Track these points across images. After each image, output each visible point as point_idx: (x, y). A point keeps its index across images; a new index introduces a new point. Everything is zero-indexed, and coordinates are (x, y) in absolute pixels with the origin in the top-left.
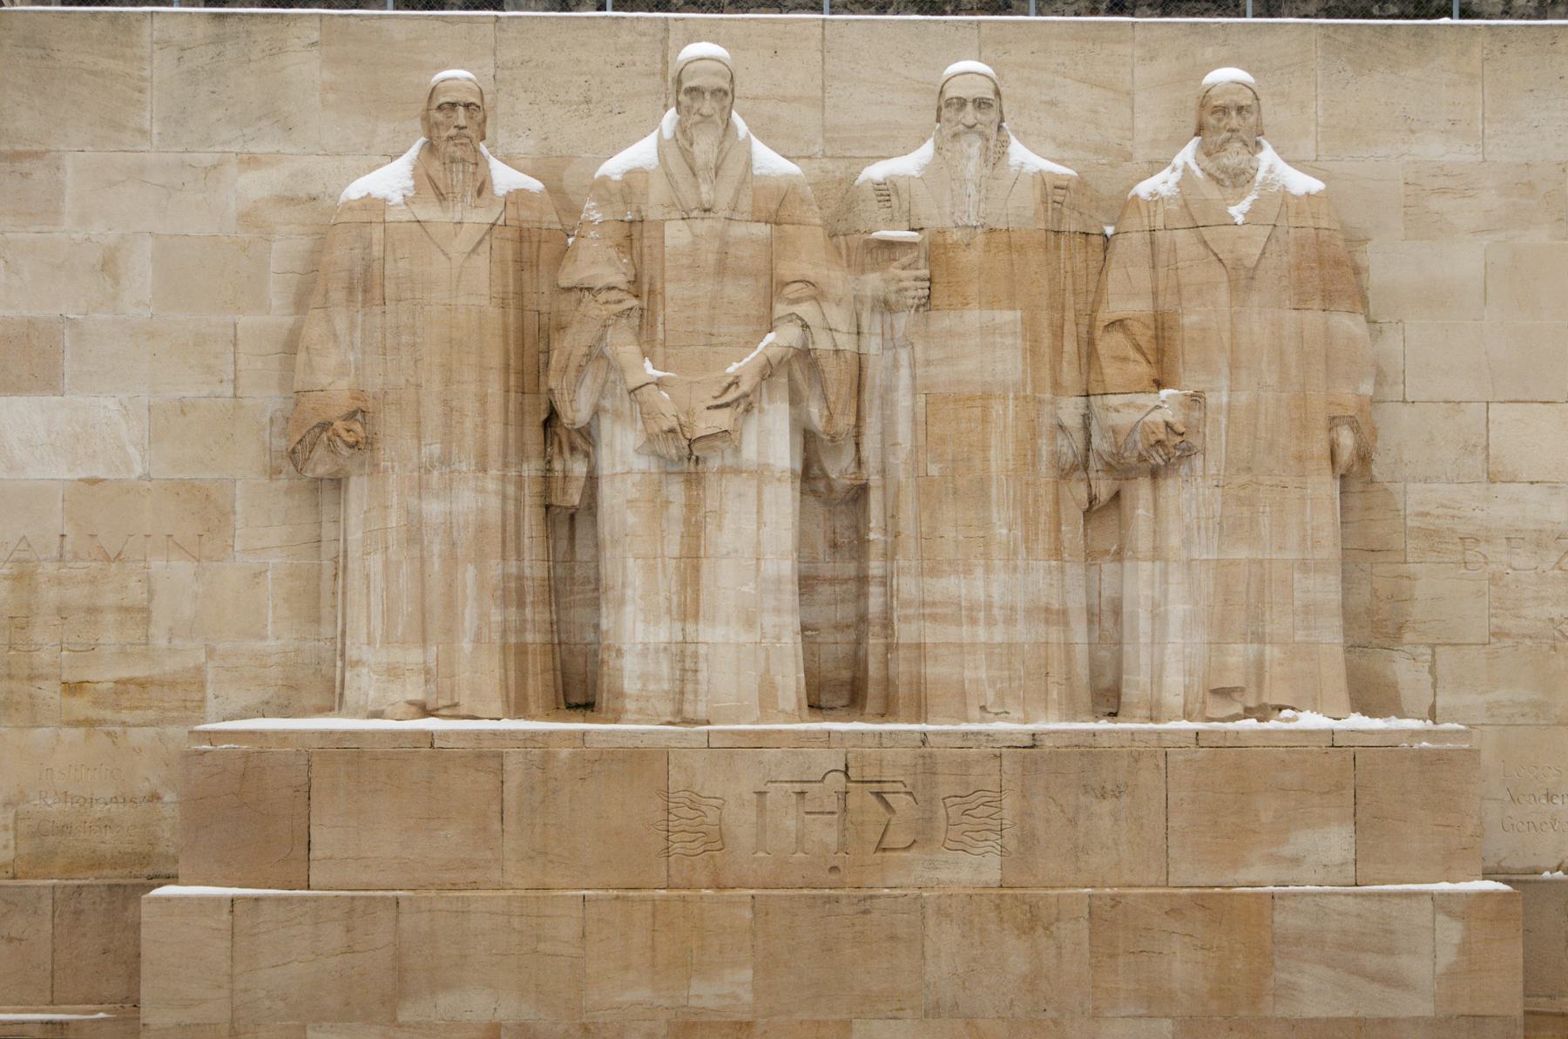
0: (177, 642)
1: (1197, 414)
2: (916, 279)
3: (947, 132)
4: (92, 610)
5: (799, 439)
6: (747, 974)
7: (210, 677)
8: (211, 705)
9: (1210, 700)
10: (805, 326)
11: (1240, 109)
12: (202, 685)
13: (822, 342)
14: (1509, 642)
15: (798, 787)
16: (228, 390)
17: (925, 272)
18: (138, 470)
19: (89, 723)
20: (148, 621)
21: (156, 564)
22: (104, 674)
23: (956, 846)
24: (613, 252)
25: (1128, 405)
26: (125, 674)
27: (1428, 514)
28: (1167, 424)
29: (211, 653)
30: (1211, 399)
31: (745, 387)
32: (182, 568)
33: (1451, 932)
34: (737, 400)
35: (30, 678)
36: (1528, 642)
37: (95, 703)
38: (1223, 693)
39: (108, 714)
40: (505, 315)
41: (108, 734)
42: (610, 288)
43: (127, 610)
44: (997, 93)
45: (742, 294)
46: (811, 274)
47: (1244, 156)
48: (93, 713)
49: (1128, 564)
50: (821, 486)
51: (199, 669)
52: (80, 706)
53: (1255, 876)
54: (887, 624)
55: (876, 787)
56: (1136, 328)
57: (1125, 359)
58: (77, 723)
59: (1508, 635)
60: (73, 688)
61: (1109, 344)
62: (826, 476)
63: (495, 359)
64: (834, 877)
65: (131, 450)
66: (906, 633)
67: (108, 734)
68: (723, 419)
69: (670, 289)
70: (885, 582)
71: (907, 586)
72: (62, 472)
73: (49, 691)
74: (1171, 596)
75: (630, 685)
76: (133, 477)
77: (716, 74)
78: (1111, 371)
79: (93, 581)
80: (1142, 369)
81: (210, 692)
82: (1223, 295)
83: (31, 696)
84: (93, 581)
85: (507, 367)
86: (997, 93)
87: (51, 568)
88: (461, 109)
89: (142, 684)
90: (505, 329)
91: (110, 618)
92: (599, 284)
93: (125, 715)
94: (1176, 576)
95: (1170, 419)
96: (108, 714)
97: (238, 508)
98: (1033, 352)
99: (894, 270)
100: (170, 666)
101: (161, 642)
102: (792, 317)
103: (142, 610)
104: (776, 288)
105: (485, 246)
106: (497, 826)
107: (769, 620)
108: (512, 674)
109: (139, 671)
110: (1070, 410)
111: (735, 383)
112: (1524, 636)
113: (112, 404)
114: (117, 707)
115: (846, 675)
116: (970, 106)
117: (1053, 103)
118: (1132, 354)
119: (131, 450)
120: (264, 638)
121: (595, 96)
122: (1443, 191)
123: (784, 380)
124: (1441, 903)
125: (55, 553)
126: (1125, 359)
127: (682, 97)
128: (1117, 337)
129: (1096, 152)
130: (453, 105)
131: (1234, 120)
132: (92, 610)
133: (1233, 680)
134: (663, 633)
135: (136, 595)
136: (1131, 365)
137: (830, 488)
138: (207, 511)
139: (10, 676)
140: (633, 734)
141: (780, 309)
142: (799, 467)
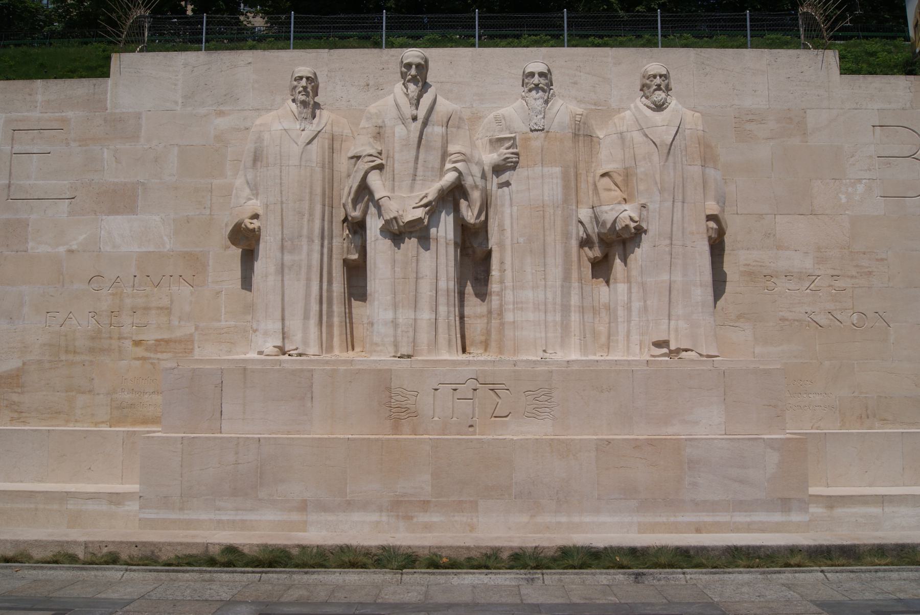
0: (182, 323)
1: (645, 213)
2: (513, 153)
3: (526, 90)
5: (459, 228)
7: (196, 338)
8: (197, 351)
9: (653, 347)
10: (460, 173)
11: (661, 76)
12: (193, 342)
13: (468, 182)
14: (787, 323)
15: (454, 386)
16: (208, 212)
17: (515, 150)
18: (168, 247)
19: (144, 359)
20: (170, 314)
21: (174, 288)
22: (150, 336)
23: (530, 415)
24: (371, 140)
25: (612, 210)
26: (160, 337)
27: (749, 265)
28: (631, 219)
29: (197, 328)
30: (651, 206)
31: (430, 198)
32: (186, 290)
33: (773, 458)
34: (425, 206)
35: (119, 339)
36: (797, 323)
37: (146, 350)
38: (658, 344)
39: (152, 355)
40: (324, 171)
41: (152, 364)
42: (371, 155)
43: (161, 308)
44: (549, 70)
45: (433, 158)
46: (463, 151)
47: (663, 95)
49: (612, 286)
50: (470, 252)
51: (191, 335)
52: (140, 352)
53: (675, 431)
54: (501, 314)
55: (492, 386)
56: (615, 175)
57: (610, 190)
59: (787, 320)
60: (137, 343)
62: (472, 247)
63: (318, 190)
64: (471, 429)
65: (165, 238)
66: (509, 317)
67: (152, 364)
68: (420, 213)
69: (397, 156)
70: (500, 294)
71: (509, 296)
72: (135, 248)
73: (128, 344)
74: (633, 299)
76: (166, 250)
77: (418, 56)
78: (604, 195)
79: (147, 296)
80: (617, 193)
81: (196, 346)
82: (656, 158)
83: (119, 347)
84: (147, 296)
85: (324, 194)
86: (549, 70)
87: (129, 290)
88: (304, 79)
89: (167, 342)
90: (324, 178)
91: (154, 312)
92: (364, 154)
93: (159, 356)
94: (634, 290)
95: (633, 215)
96: (152, 355)
97: (211, 263)
98: (566, 187)
99: (503, 150)
100: (178, 334)
102: (455, 169)
103: (167, 309)
104: (445, 155)
105: (316, 141)
106: (309, 404)
107: (442, 309)
108: (324, 335)
109: (166, 336)
110: (584, 214)
111: (426, 196)
112: (794, 320)
113: (157, 218)
114: (156, 352)
115: (483, 338)
116: (536, 76)
117: (575, 83)
118: (613, 187)
119: (165, 238)
120: (220, 321)
121: (371, 83)
122: (751, 121)
123: (451, 199)
124: (771, 444)
125: (131, 284)
126: (610, 190)
127: (404, 69)
128: (606, 179)
129: (595, 104)
130: (301, 78)
131: (658, 80)
132: (147, 309)
133: (663, 337)
134: (389, 315)
135: (166, 302)
136: (613, 193)
137: (474, 252)
138: (194, 265)
139: (111, 338)
140: (375, 361)
141: (448, 166)
142: (459, 241)
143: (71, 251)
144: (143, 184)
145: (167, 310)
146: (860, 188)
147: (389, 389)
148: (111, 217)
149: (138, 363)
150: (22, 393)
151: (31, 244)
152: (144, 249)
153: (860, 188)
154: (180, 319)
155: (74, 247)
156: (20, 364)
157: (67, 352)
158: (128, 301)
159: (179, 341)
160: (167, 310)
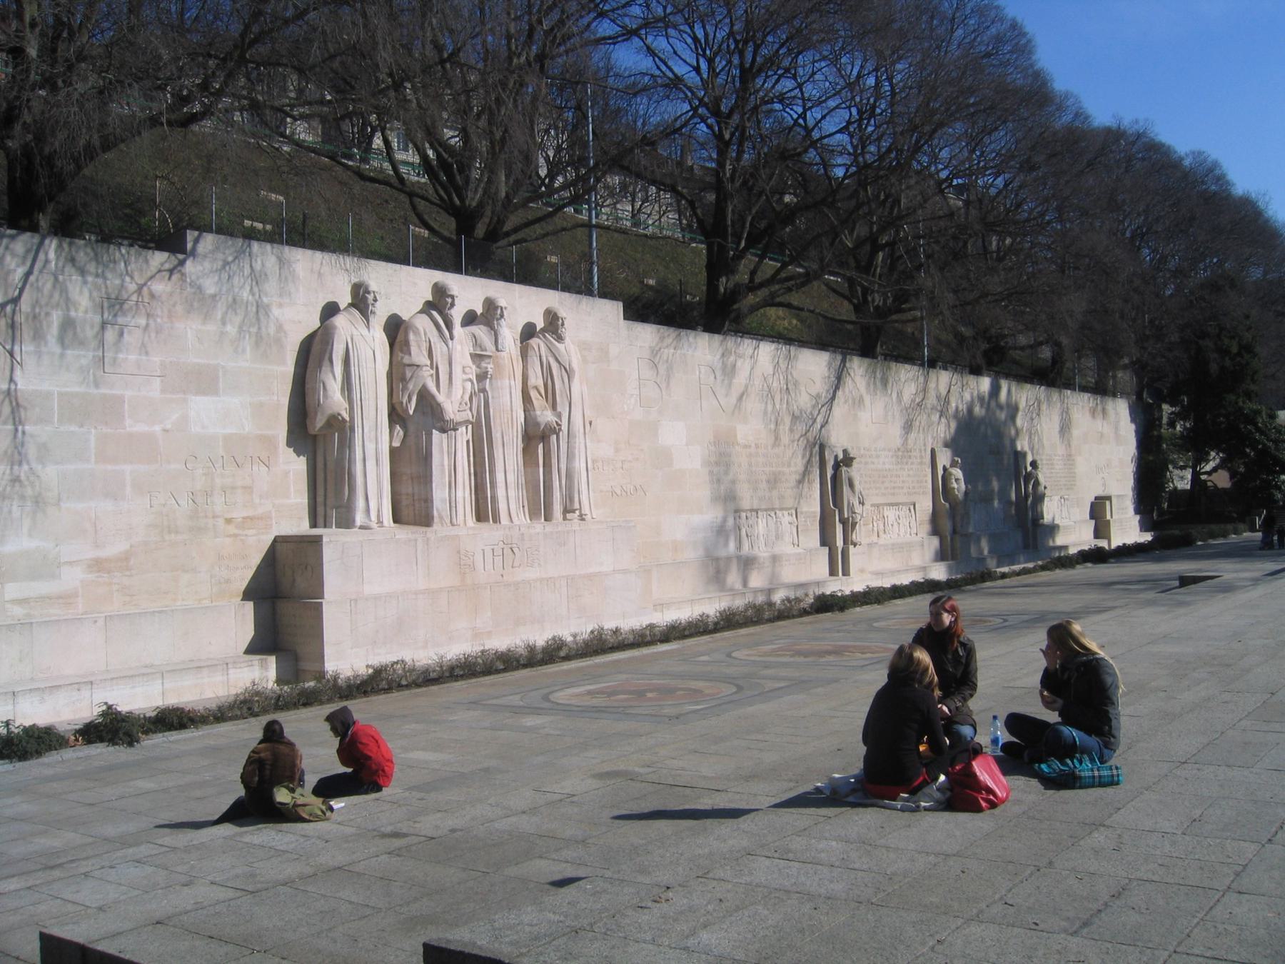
4: (233, 488)
6: (489, 614)
19: (236, 536)
22: (238, 514)
26: (245, 514)
48: (236, 531)
52: (232, 529)
58: (229, 536)
60: (229, 521)
61: (533, 394)
73: (221, 522)
75: (435, 513)
89: (251, 518)
93: (247, 532)
100: (260, 511)
101: (257, 501)
109: (250, 513)
143: (166, 431)
144: (223, 367)
145: (248, 489)
146: (633, 401)
147: (459, 552)
148: (198, 398)
149: (228, 540)
150: (131, 576)
151: (128, 422)
152: (229, 431)
153: (633, 401)
154: (261, 497)
155: (169, 427)
156: (128, 547)
157: (170, 532)
158: (218, 481)
159: (260, 518)
160: (248, 489)
